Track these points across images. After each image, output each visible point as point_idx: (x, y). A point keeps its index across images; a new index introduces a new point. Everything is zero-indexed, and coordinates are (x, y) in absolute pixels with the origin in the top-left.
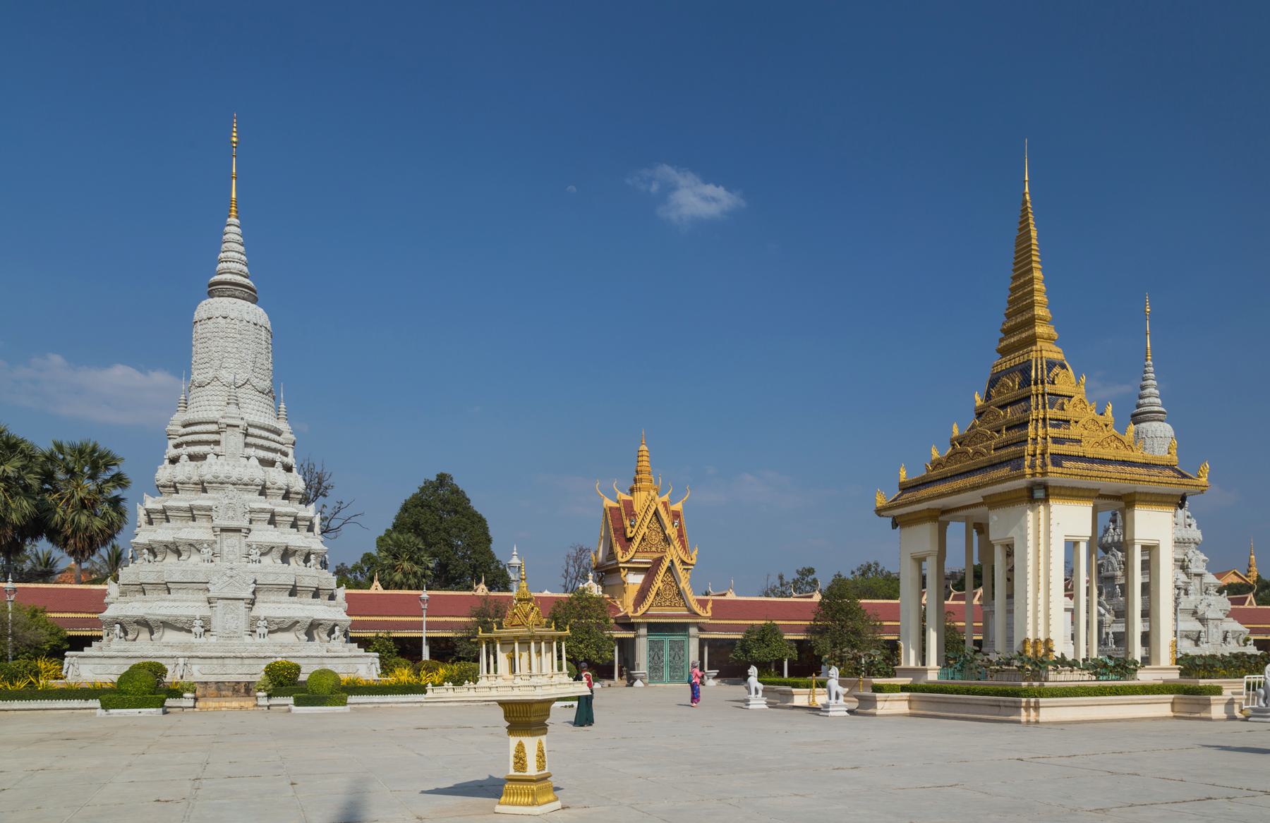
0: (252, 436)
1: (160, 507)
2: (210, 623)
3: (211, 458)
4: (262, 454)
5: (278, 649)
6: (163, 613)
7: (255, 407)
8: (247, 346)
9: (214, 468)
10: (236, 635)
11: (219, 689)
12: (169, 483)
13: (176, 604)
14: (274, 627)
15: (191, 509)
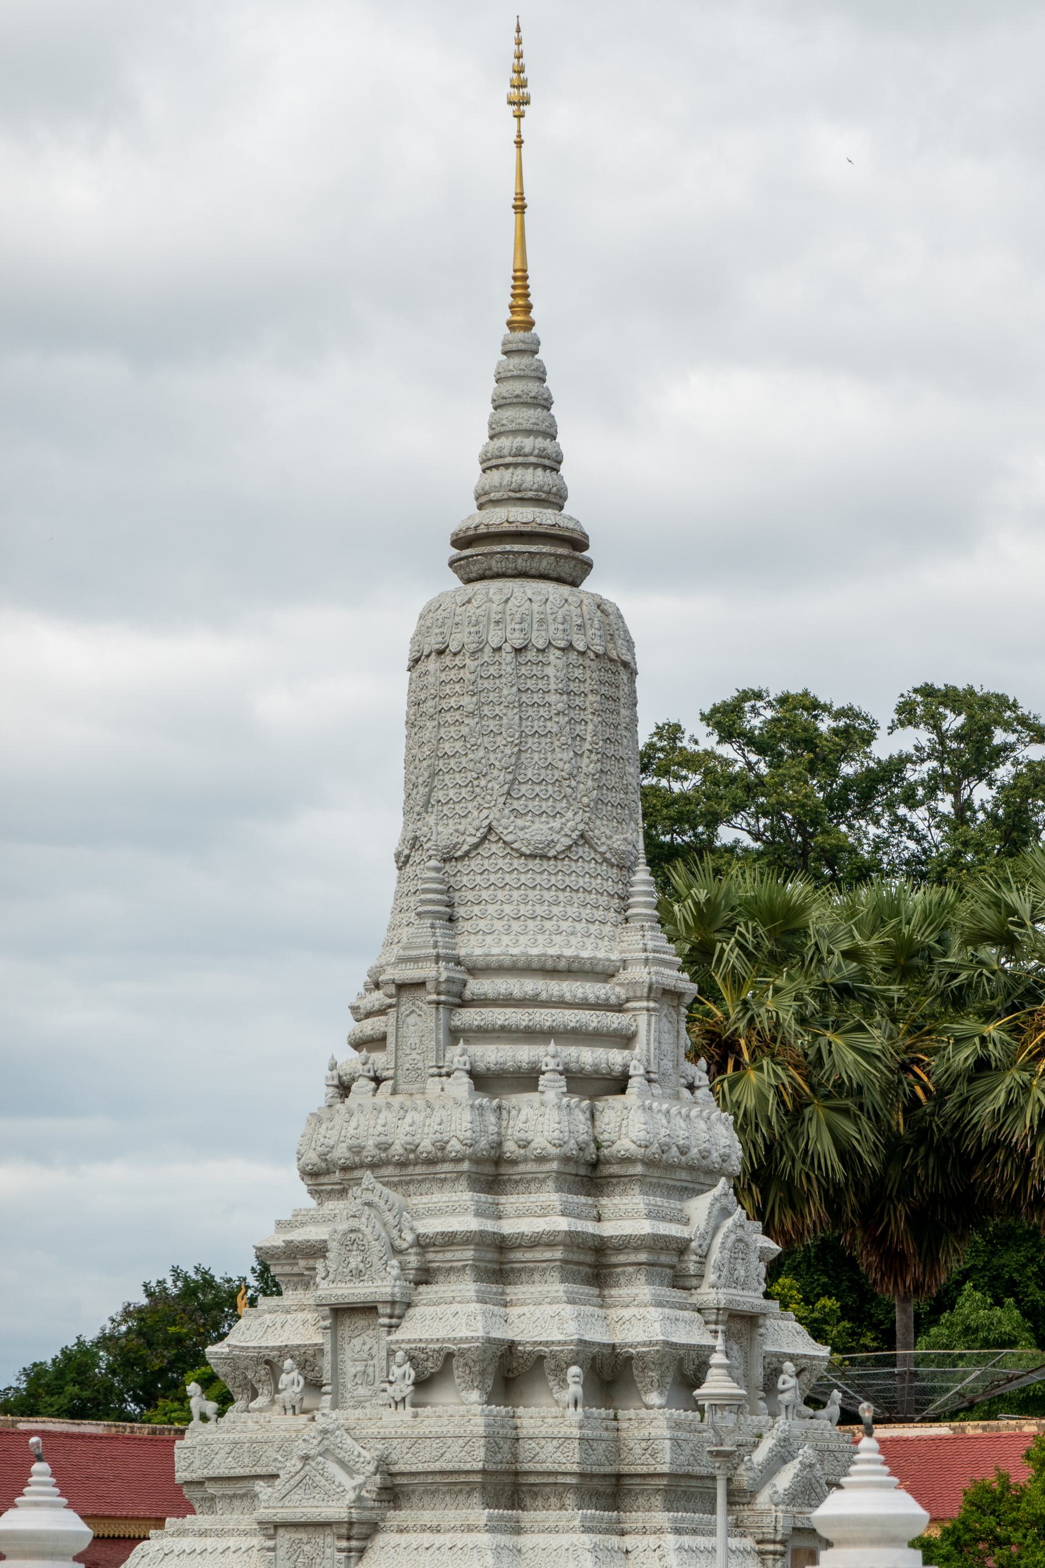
8: (492, 724)
9: (353, 1123)
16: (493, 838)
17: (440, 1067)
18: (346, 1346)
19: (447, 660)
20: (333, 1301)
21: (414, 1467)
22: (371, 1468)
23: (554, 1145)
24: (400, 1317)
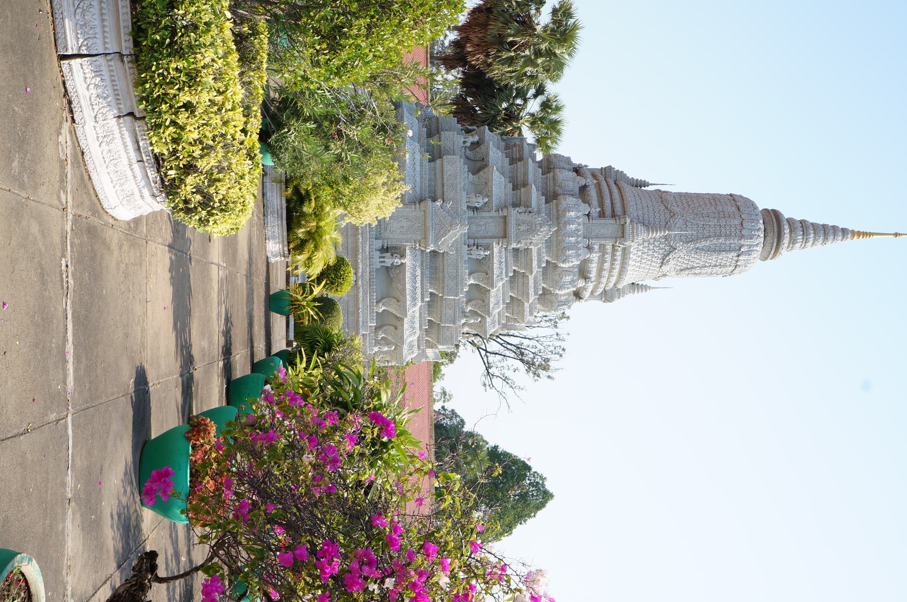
3: (585, 209)
10: (382, 231)
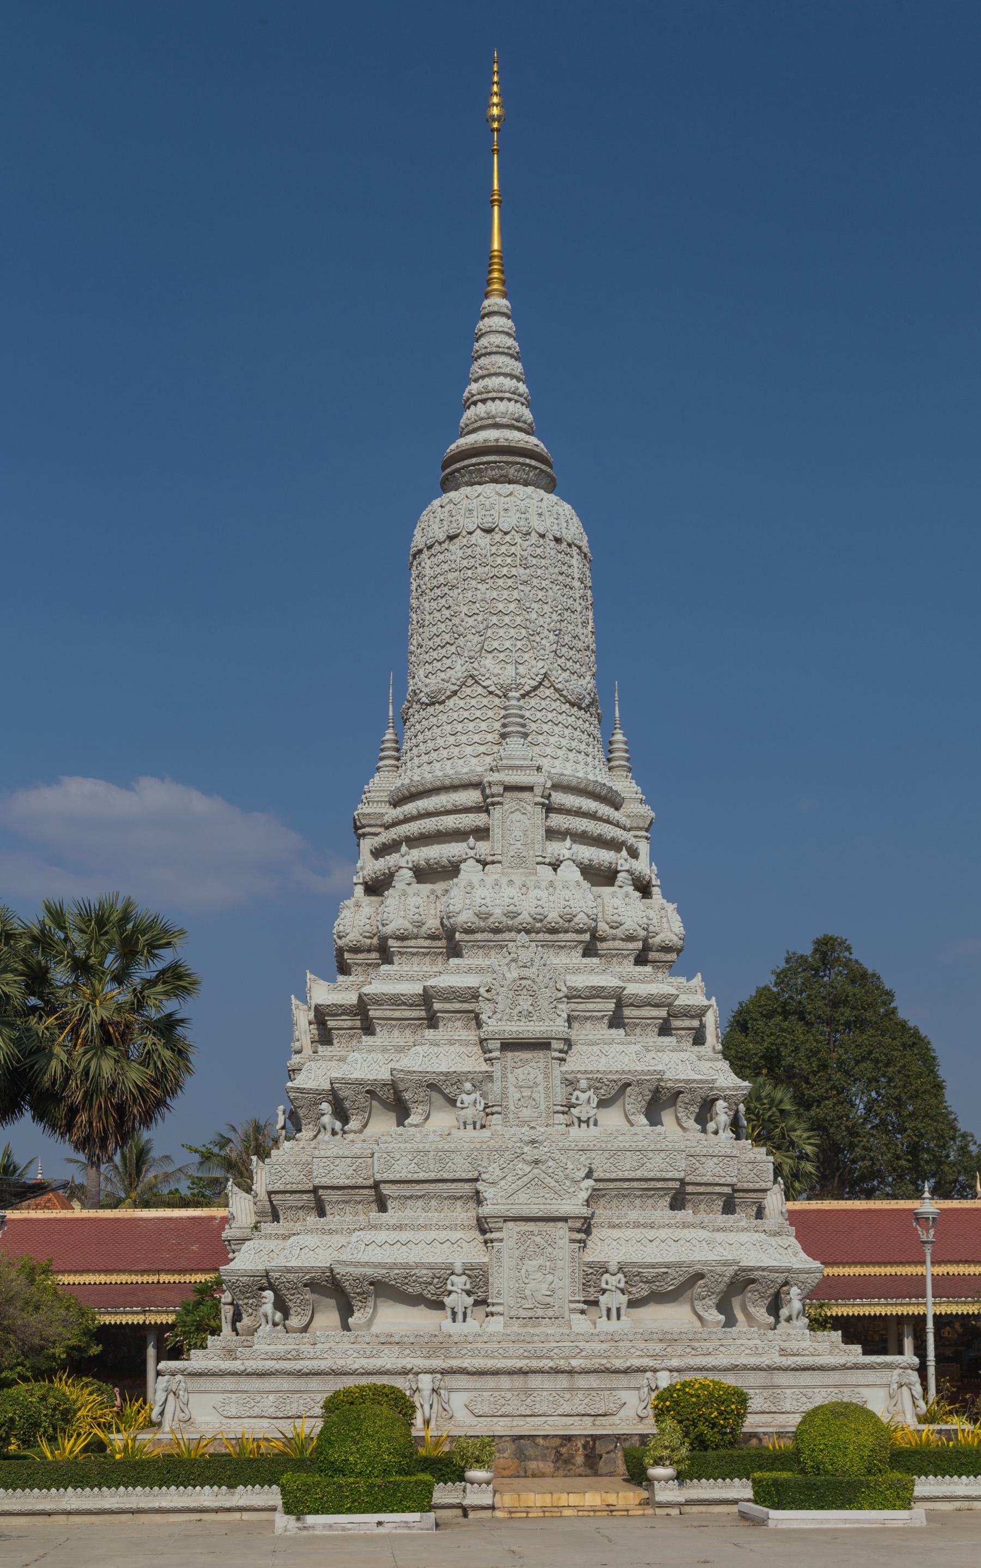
0: (562, 810)
1: (351, 998)
2: (486, 1283)
3: (469, 871)
4: (587, 853)
5: (657, 1347)
6: (373, 1260)
7: (564, 742)
8: (541, 594)
9: (479, 893)
10: (550, 1313)
11: (521, 1456)
12: (368, 941)
13: (405, 1236)
14: (642, 1290)
15: (427, 998)
16: (546, 683)
17: (545, 857)
18: (509, 1075)
19: (497, 537)
20: (507, 1035)
21: (614, 1174)
22: (582, 1174)
23: (644, 929)
24: (566, 1052)
